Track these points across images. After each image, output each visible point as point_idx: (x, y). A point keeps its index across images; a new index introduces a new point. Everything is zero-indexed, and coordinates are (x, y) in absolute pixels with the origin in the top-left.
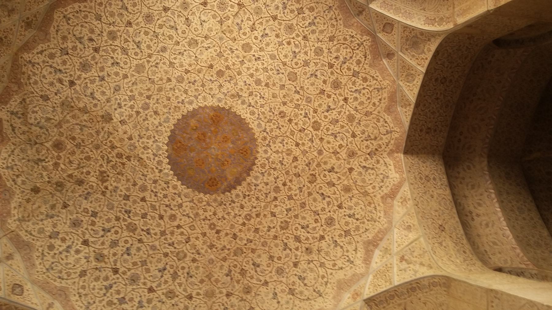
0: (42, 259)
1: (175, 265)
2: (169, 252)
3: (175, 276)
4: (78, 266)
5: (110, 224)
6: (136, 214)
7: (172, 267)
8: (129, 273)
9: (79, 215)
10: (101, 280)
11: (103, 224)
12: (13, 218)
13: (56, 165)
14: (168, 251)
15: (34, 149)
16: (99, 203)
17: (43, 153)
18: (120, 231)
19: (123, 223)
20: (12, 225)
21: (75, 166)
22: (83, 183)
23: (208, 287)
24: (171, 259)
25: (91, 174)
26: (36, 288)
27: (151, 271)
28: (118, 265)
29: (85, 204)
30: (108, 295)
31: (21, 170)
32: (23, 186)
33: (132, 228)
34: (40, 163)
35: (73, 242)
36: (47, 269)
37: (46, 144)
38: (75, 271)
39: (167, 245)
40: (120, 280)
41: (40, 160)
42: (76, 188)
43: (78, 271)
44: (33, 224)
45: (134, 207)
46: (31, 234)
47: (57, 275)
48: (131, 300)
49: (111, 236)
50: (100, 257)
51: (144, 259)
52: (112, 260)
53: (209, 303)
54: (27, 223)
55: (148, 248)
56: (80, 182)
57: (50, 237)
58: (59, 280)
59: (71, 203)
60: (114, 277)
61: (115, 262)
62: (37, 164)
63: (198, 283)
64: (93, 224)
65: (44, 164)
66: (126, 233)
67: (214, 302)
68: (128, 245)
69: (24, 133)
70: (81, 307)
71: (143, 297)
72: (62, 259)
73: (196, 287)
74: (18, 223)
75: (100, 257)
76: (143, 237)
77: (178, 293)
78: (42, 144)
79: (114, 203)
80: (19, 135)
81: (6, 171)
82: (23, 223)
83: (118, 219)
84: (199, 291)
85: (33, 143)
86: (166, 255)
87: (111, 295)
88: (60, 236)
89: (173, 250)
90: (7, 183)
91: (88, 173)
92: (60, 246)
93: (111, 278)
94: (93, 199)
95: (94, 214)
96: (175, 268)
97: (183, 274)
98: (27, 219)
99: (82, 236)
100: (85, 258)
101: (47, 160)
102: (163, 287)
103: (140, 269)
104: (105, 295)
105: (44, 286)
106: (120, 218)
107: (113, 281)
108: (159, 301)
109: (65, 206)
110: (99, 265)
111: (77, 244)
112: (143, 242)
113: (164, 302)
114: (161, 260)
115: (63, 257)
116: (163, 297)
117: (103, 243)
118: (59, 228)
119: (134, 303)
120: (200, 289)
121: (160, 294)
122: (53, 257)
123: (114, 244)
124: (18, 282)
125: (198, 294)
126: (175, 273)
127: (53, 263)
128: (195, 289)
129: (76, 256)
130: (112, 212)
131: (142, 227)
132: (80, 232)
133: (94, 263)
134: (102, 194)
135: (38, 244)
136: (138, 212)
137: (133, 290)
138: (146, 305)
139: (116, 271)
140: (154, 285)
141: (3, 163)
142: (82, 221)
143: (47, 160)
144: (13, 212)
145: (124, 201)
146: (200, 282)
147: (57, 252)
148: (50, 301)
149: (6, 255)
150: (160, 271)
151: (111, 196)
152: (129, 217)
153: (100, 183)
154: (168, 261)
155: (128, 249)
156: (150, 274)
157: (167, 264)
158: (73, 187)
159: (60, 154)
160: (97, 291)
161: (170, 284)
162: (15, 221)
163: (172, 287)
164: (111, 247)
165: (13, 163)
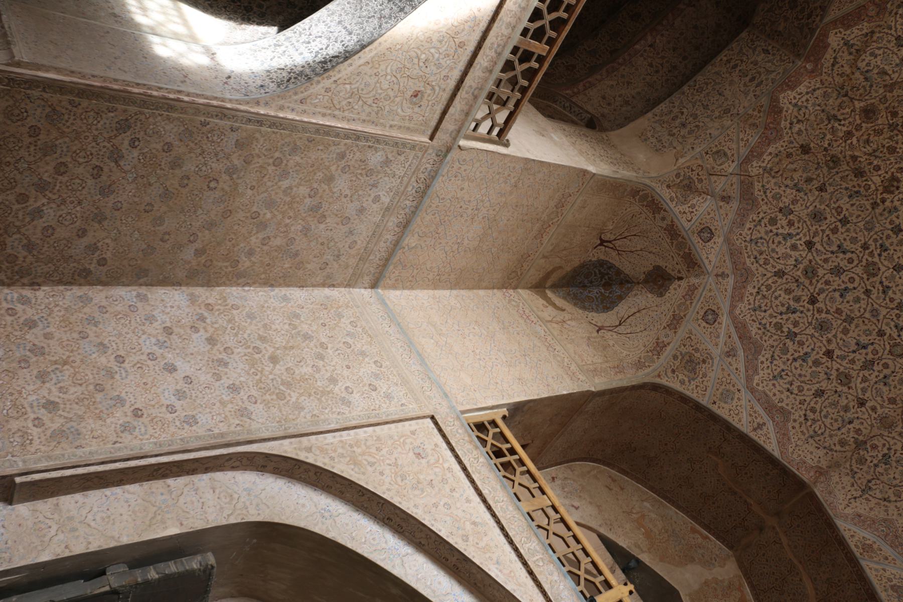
0: (755, 226)
1: (880, 354)
2: (888, 334)
3: (868, 365)
4: (781, 262)
5: (852, 245)
6: (890, 258)
7: (875, 352)
8: (823, 315)
9: (828, 210)
10: (791, 296)
11: (845, 239)
12: (760, 164)
13: (849, 134)
14: (888, 331)
15: (839, 101)
16: (860, 213)
17: (845, 111)
18: (856, 262)
19: (866, 256)
20: (754, 170)
21: (869, 149)
22: (862, 176)
23: (891, 413)
24: (882, 343)
25: (880, 173)
26: (725, 248)
27: (849, 335)
28: (821, 298)
29: (844, 203)
30: (784, 317)
31: (807, 116)
32: (796, 136)
33: (871, 270)
34: (832, 122)
35: (798, 234)
36: (751, 240)
37: (856, 102)
38: (775, 264)
39: (893, 323)
40: (809, 314)
41: (835, 116)
42: (849, 177)
43: (779, 267)
44: (775, 184)
45: (897, 248)
46: (765, 193)
47: (755, 253)
48: (801, 344)
49: (840, 260)
50: (810, 272)
51: (853, 315)
52: (819, 286)
53: (875, 431)
54: (770, 179)
55: (869, 308)
56: (859, 173)
57: (781, 210)
58: (752, 260)
59: (830, 189)
60: (807, 305)
61: (822, 291)
62: (829, 120)
63: (885, 397)
64: (835, 231)
65: (836, 125)
66: (859, 270)
67: (881, 435)
68: (850, 286)
69: (842, 75)
70: (750, 304)
71: (815, 352)
72: (773, 242)
73: (879, 399)
74: (761, 170)
75: (810, 272)
76: (875, 291)
77: (852, 385)
78: (852, 99)
79: (877, 225)
80: (835, 75)
81: (791, 108)
82: (766, 175)
83: (865, 247)
84: (878, 407)
85: (843, 92)
86: (881, 333)
87: (787, 320)
88: (791, 217)
89: (895, 335)
90: (783, 122)
91: (877, 168)
92: (782, 227)
93: (801, 303)
94: (858, 203)
95: (845, 221)
96: (876, 357)
97: (879, 371)
98: (773, 174)
99: (812, 235)
100: (796, 260)
101: (843, 122)
102: (844, 363)
103: (839, 322)
104: (781, 314)
105: (734, 254)
106: (868, 248)
107: (802, 309)
108: (826, 374)
109: (822, 189)
110: (802, 280)
111: (800, 239)
112: (869, 297)
113: (829, 379)
114: (870, 334)
115: (776, 241)
116: (834, 373)
117: (826, 261)
118: (797, 208)
119: (800, 349)
120: (882, 406)
121: (835, 367)
122: (767, 233)
123: (837, 271)
124: (713, 228)
125: (874, 409)
126: (872, 362)
127: (761, 238)
128: (876, 401)
129: (788, 251)
130: (866, 233)
131: (884, 280)
132: (814, 228)
133: (799, 273)
134: (872, 204)
135: (764, 208)
136: (895, 257)
137: (812, 336)
138: (810, 363)
139: (813, 301)
140: (837, 352)
141: (795, 98)
142: (826, 219)
143: (843, 122)
144: (765, 157)
145: (890, 232)
146: (889, 399)
147: (775, 231)
148: (727, 272)
149: (725, 194)
150: (857, 344)
151: (881, 215)
152: (880, 255)
153: (881, 188)
154: (876, 341)
155: (846, 289)
156: (844, 337)
157: (872, 344)
158: (847, 172)
159: (863, 125)
160: (777, 302)
161: (855, 367)
162: (760, 167)
163: (854, 374)
164: (831, 271)
165: (805, 104)
